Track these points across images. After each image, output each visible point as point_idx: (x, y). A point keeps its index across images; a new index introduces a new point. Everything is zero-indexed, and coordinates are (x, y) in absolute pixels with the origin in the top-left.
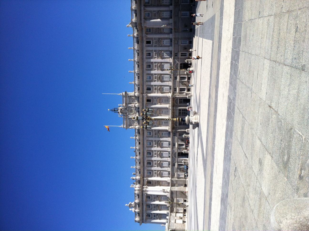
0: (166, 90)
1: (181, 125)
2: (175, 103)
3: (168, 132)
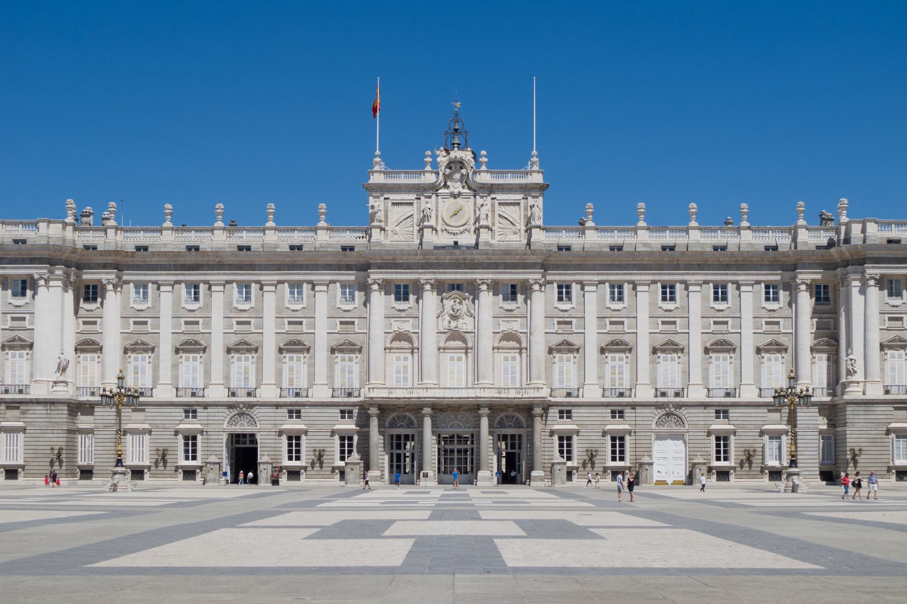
0: (561, 373)
1: (392, 448)
2: (503, 415)
3: (356, 385)
